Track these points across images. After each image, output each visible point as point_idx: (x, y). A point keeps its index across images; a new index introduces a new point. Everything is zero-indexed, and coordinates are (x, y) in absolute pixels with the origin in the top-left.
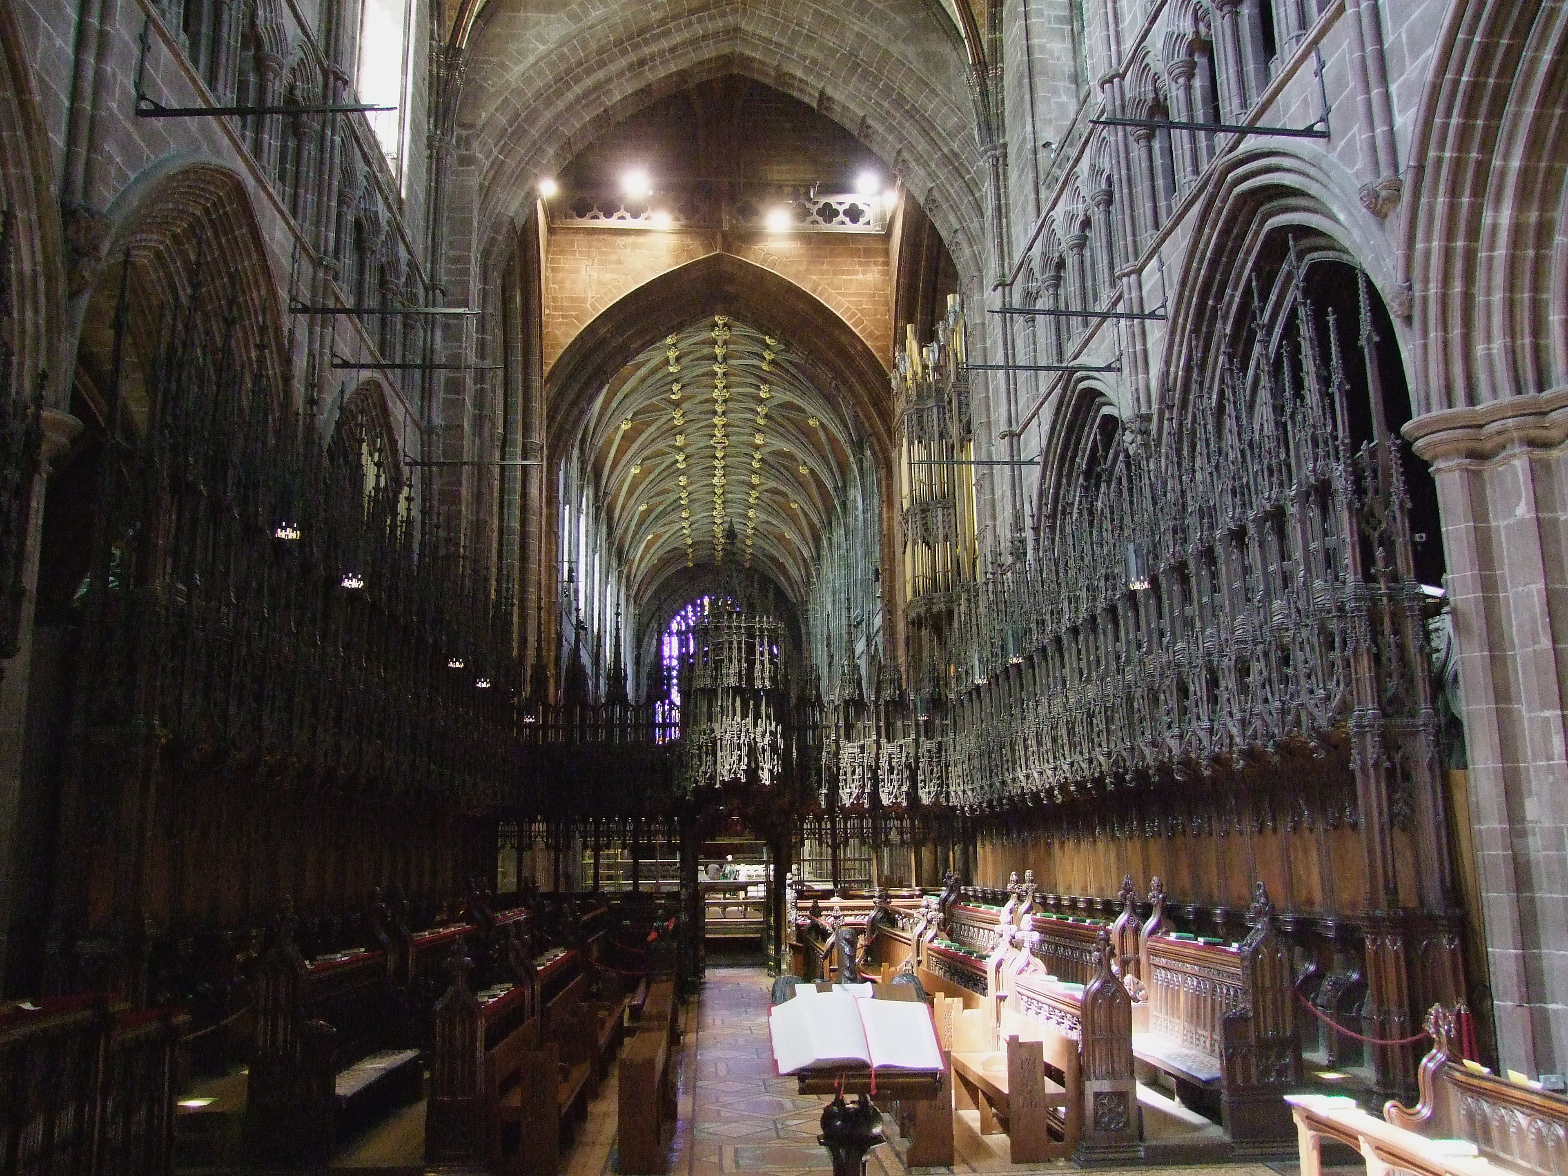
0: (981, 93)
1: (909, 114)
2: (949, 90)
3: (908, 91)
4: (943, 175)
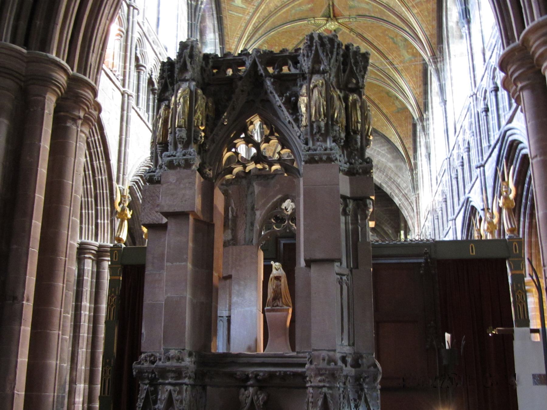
0: (412, 178)
1: (393, 182)
2: (403, 176)
3: (392, 176)
4: (403, 200)
